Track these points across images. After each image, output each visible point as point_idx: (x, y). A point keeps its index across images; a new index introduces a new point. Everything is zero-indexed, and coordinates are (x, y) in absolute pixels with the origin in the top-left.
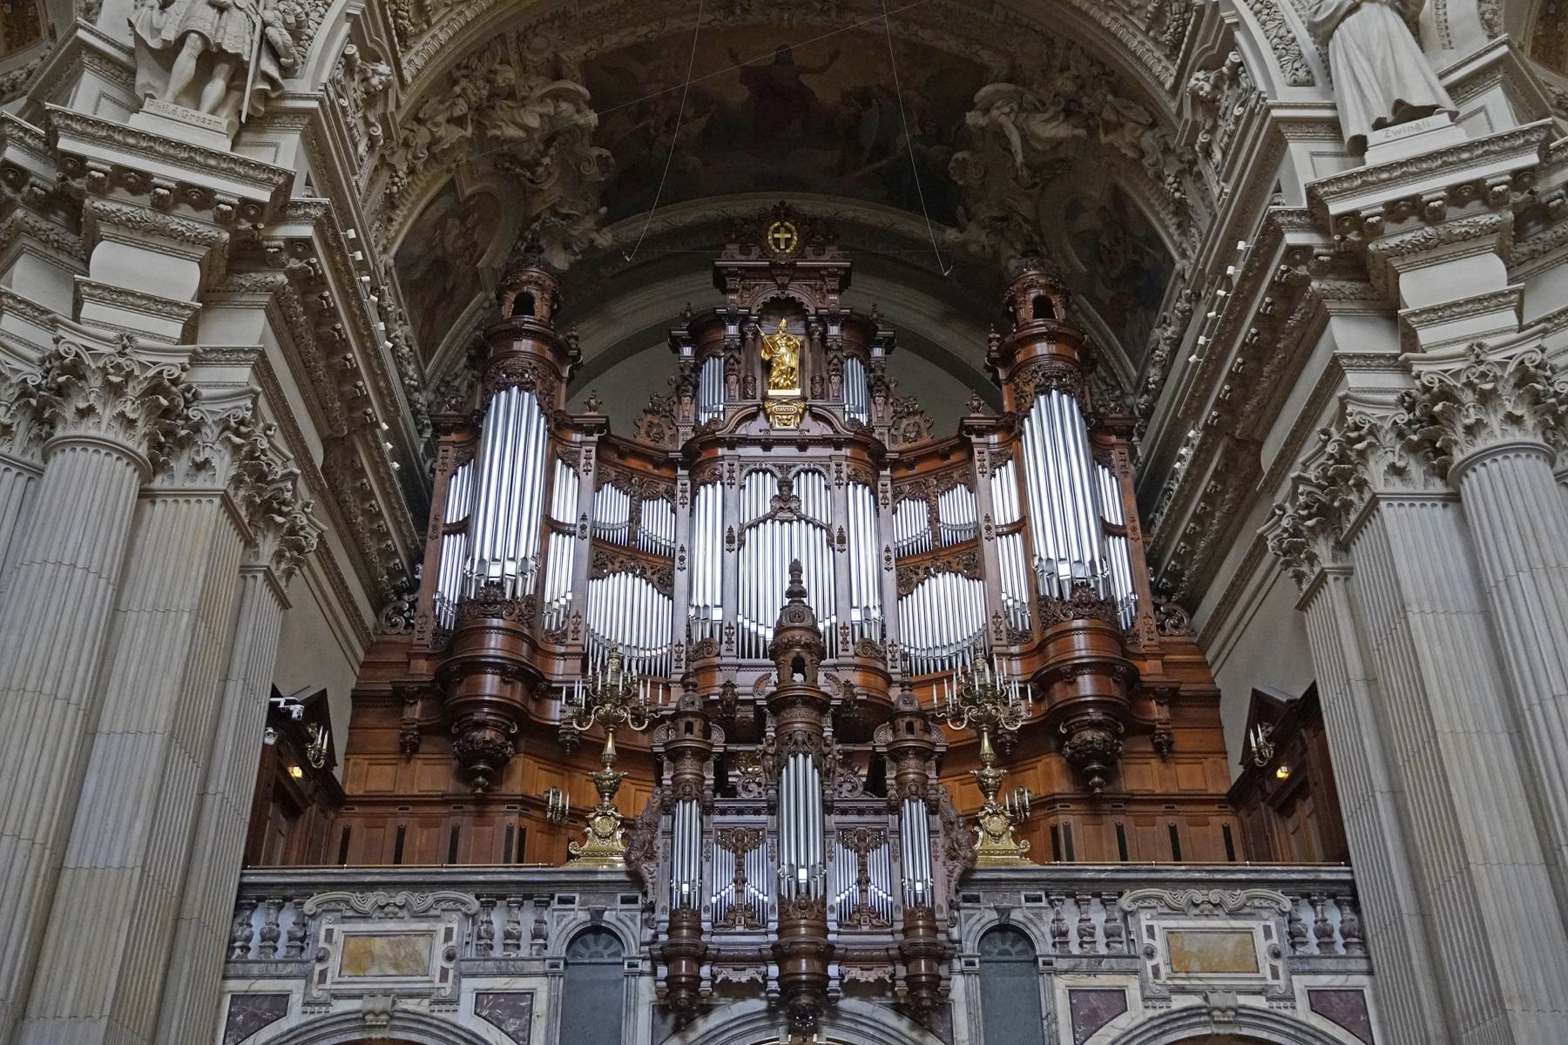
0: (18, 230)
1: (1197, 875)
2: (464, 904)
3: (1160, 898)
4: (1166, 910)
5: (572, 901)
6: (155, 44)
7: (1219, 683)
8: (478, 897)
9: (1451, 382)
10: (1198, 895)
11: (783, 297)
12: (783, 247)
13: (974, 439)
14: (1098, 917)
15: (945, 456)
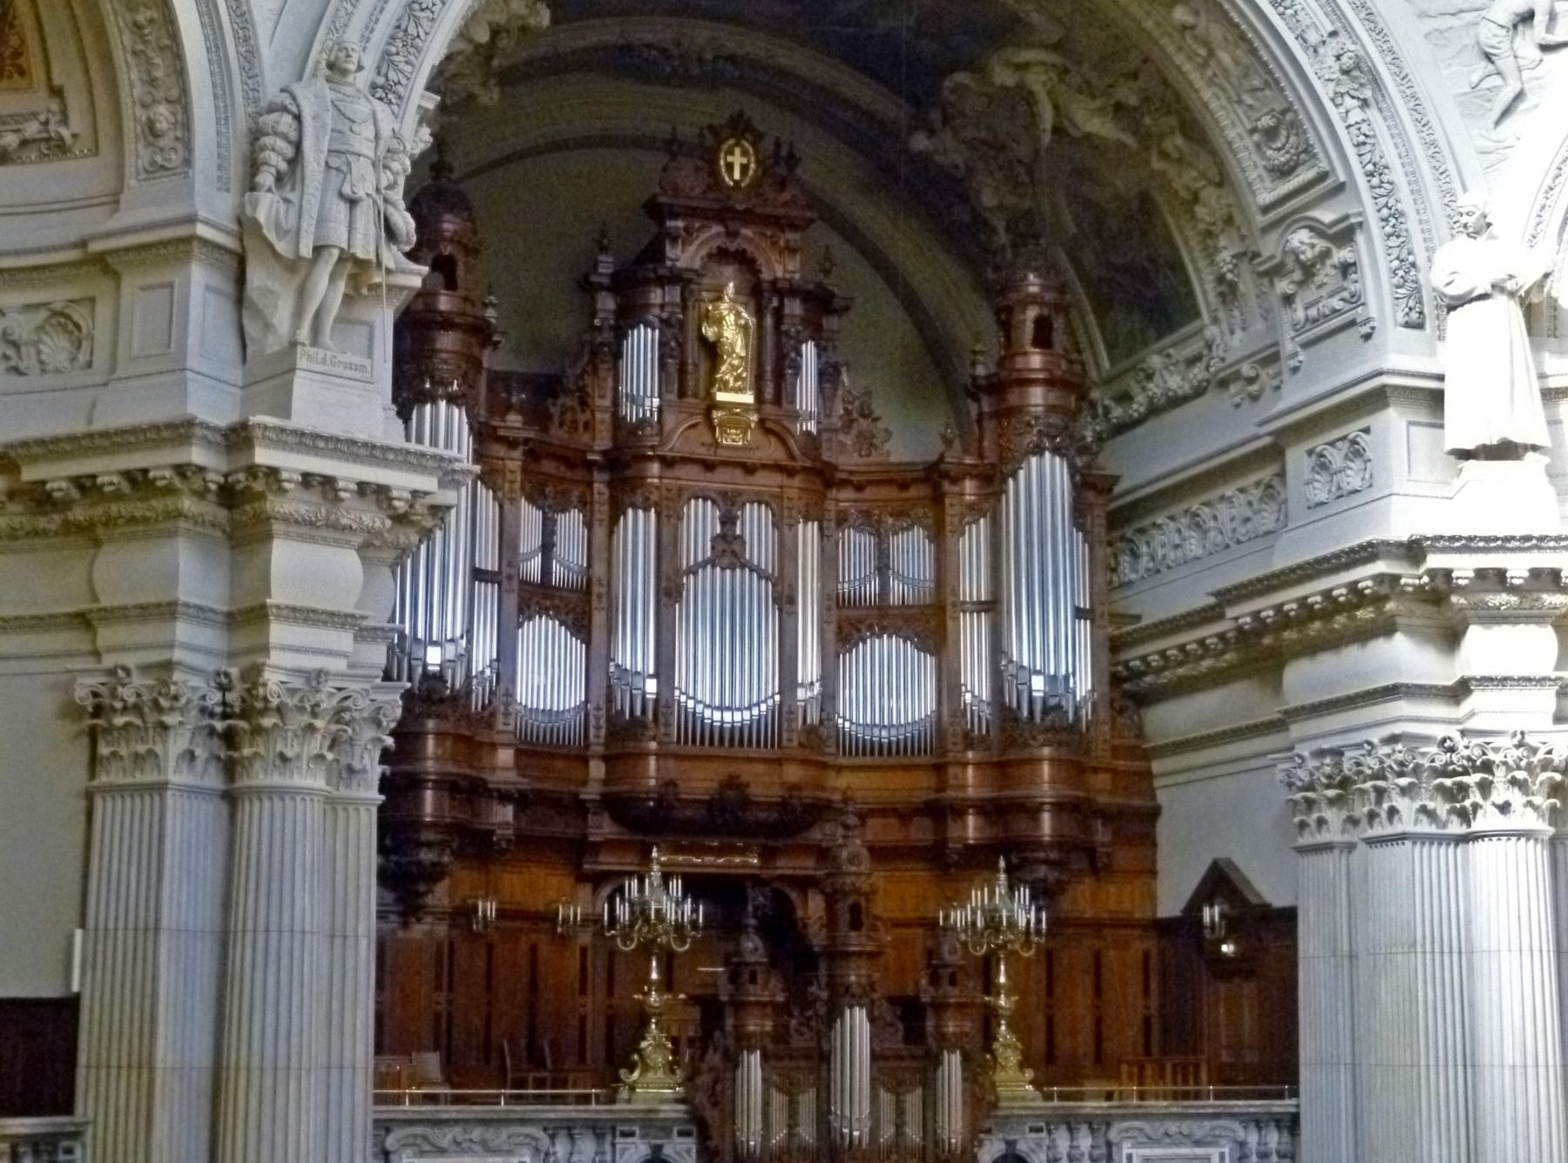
0: (179, 514)
1: (1174, 1110)
2: (534, 1138)
3: (1140, 1130)
4: (1144, 1140)
5: (632, 1134)
6: (282, 247)
7: (1162, 797)
8: (545, 1129)
9: (1491, 756)
10: (1173, 1127)
11: (732, 247)
12: (737, 175)
13: (947, 486)
14: (1085, 1142)
15: (903, 486)
